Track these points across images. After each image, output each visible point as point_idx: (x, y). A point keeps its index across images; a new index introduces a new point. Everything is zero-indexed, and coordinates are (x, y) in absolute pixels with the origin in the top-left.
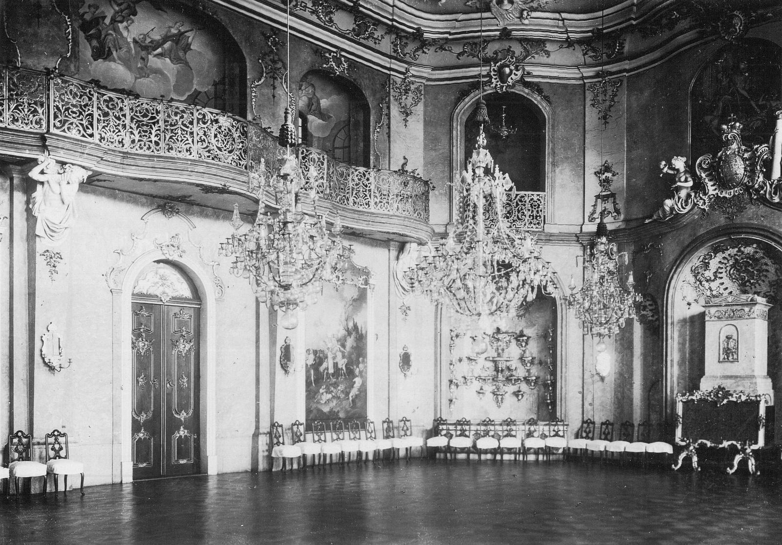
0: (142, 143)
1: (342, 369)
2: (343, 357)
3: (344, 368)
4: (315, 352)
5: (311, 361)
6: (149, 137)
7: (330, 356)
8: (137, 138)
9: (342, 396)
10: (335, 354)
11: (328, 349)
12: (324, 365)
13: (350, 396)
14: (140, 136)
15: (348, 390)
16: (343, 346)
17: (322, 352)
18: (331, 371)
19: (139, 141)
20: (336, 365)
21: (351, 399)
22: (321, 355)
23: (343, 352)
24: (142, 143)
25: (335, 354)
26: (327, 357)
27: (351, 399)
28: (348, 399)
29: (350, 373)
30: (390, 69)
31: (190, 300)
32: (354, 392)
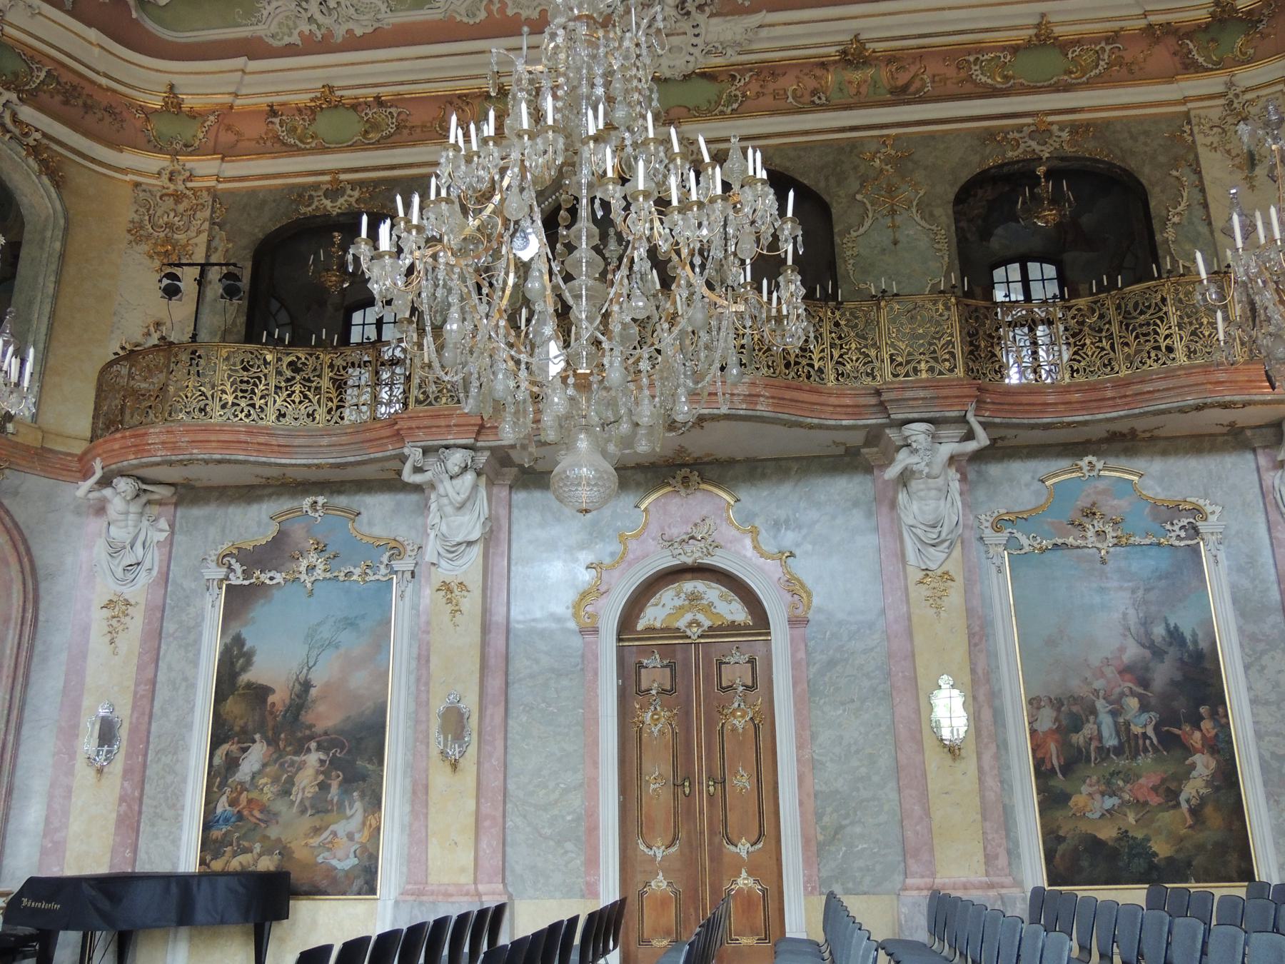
0: (239, 409)
1: (1145, 735)
2: (1144, 707)
3: (1150, 733)
4: (1057, 704)
5: (1047, 721)
6: (251, 398)
7: (1100, 705)
8: (230, 399)
9: (1155, 800)
10: (1118, 701)
11: (1096, 692)
12: (1089, 729)
13: (1182, 798)
14: (236, 397)
15: (1173, 786)
16: (1145, 683)
17: (1075, 700)
18: (1111, 741)
19: (234, 404)
20: (1123, 730)
21: (1185, 806)
22: (1075, 709)
23: (1141, 698)
24: (239, 409)
25: (1118, 701)
26: (1094, 711)
27: (1185, 806)
28: (1178, 805)
29: (1170, 743)
30: (1185, 100)
31: (747, 627)
32: (1193, 788)
